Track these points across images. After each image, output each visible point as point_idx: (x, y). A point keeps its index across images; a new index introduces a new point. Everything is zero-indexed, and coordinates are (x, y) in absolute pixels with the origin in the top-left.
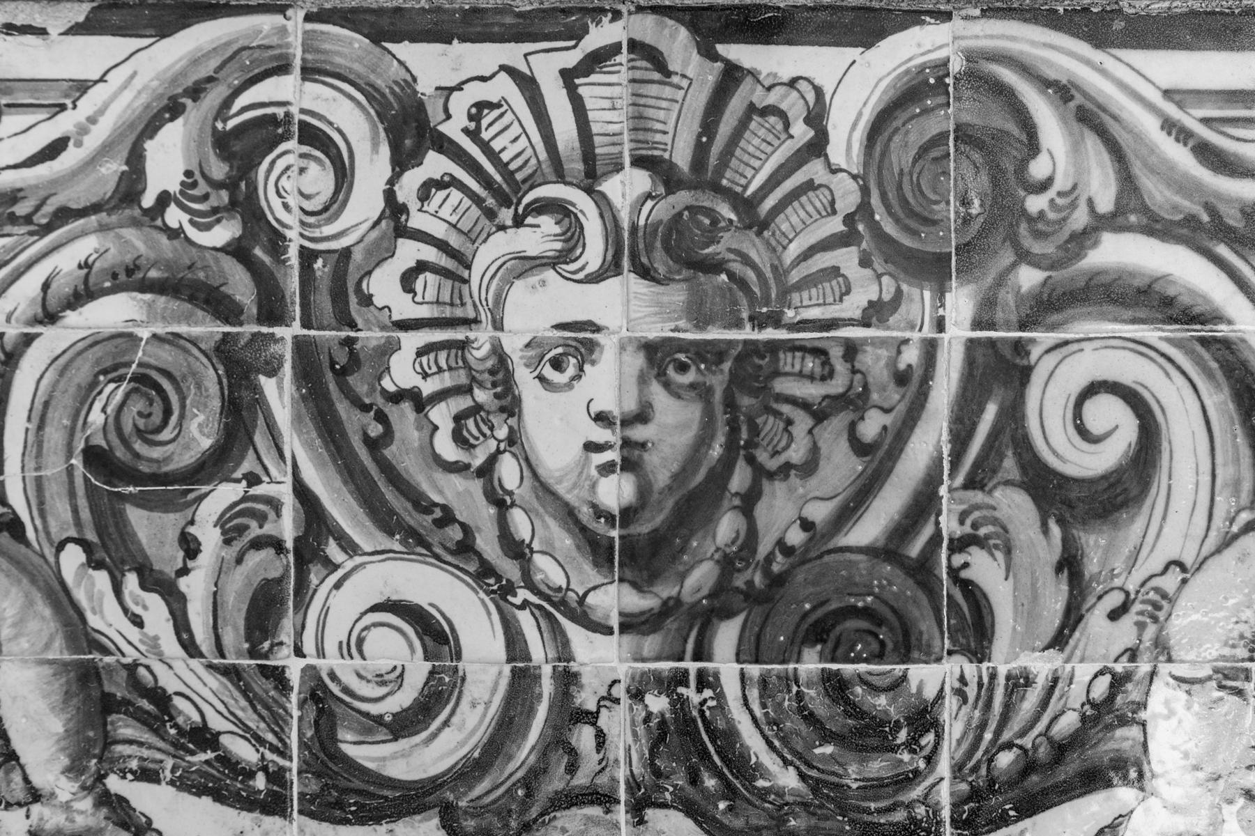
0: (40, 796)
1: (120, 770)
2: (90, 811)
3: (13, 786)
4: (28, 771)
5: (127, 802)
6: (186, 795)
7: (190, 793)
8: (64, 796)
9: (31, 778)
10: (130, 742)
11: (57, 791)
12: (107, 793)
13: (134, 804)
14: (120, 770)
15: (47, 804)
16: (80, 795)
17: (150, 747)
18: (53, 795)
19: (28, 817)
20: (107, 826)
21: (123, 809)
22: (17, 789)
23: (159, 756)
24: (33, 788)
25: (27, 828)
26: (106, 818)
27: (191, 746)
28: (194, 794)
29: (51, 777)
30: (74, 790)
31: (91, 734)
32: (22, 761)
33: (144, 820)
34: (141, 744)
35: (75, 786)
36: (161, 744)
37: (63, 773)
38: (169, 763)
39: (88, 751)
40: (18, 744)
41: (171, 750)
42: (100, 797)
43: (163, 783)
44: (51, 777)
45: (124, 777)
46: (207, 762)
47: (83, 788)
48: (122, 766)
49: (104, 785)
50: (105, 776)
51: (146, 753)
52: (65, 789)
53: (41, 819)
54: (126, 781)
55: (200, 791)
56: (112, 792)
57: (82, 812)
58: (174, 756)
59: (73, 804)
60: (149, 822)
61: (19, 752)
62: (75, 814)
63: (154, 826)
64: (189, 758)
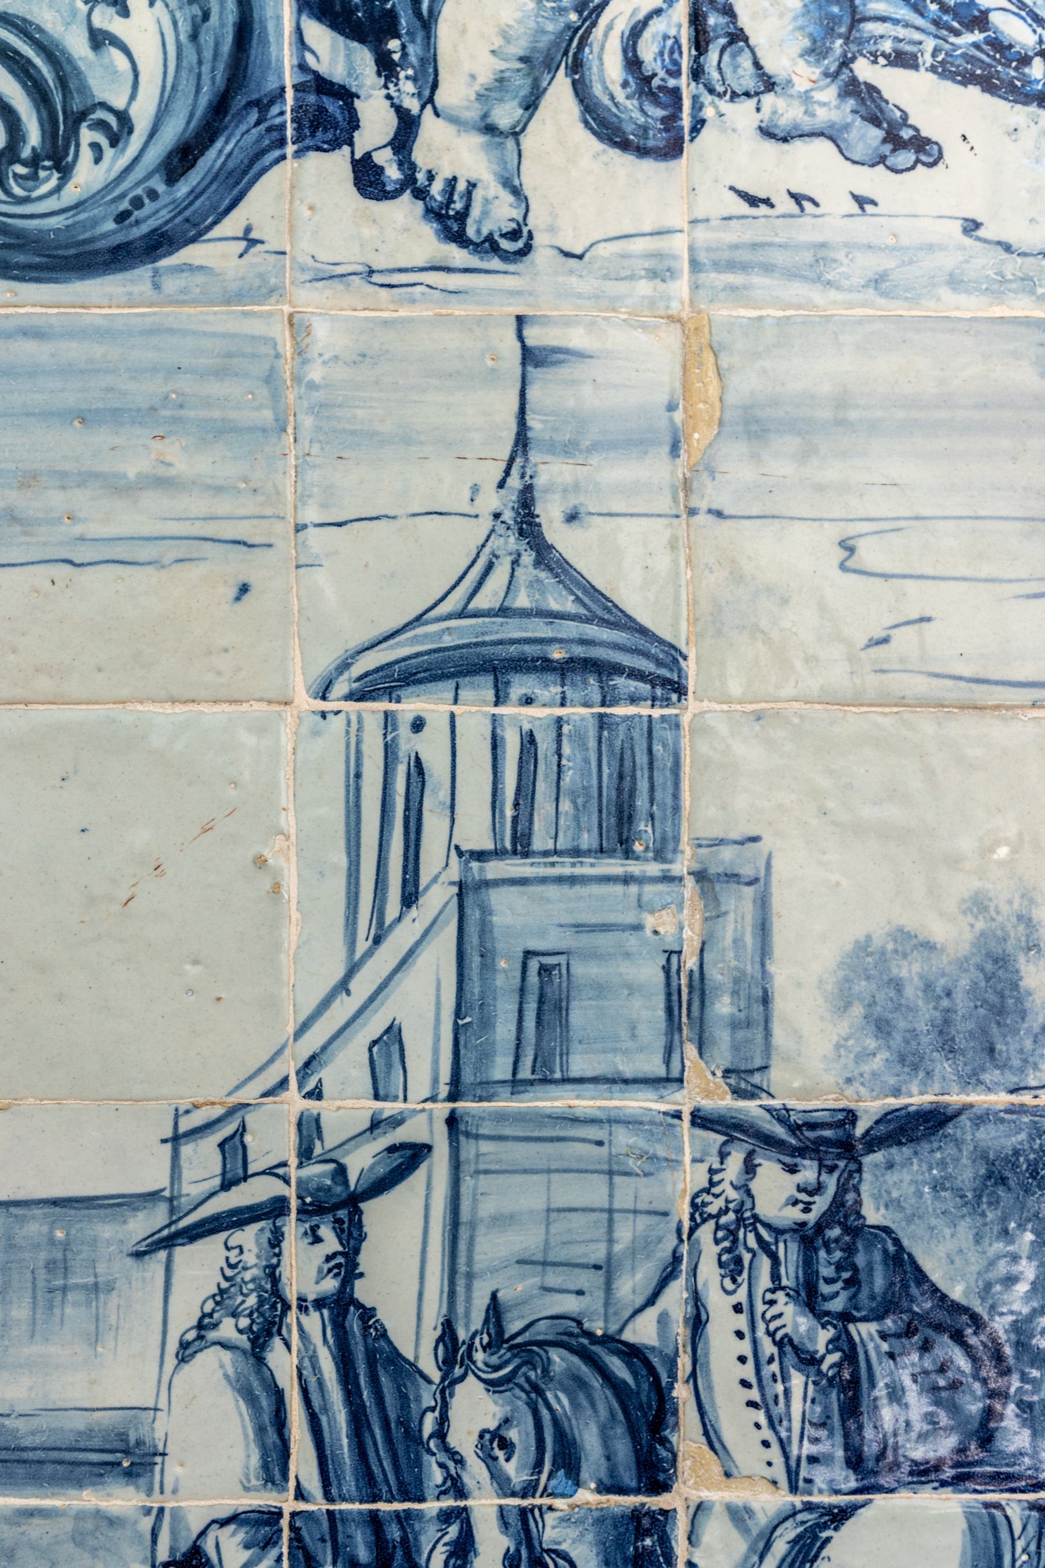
0: (774, 84)
1: (871, 53)
2: (834, 103)
3: (740, 71)
4: (759, 54)
5: (878, 92)
6: (949, 84)
7: (954, 81)
8: (801, 85)
9: (762, 62)
10: (883, 19)
11: (795, 79)
12: (854, 81)
13: (886, 95)
14: (871, 53)
15: (783, 94)
16: (822, 83)
17: (907, 25)
18: (789, 82)
19: (758, 110)
20: (854, 121)
21: (873, 101)
22: (745, 77)
23: (917, 36)
24: (764, 74)
25: (756, 124)
26: (854, 112)
27: (955, 24)
28: (961, 83)
29: (785, 62)
30: (814, 77)
31: (835, 9)
32: (751, 42)
33: (898, 114)
34: (896, 22)
35: (816, 72)
36: (919, 21)
37: (802, 56)
38: (930, 44)
39: (833, 29)
40: (744, 20)
41: (932, 28)
42: (847, 85)
43: (922, 69)
44: (785, 62)
45: (875, 62)
46: (976, 46)
47: (826, 75)
48: (873, 48)
49: (851, 71)
50: (854, 59)
51: (901, 32)
52: (803, 74)
53: (774, 112)
54: (878, 67)
55: (967, 79)
56: (861, 79)
57: (824, 104)
58: (936, 37)
59: (813, 94)
60: (905, 116)
61: (748, 32)
62: (816, 107)
63: (910, 122)
64: (953, 39)
